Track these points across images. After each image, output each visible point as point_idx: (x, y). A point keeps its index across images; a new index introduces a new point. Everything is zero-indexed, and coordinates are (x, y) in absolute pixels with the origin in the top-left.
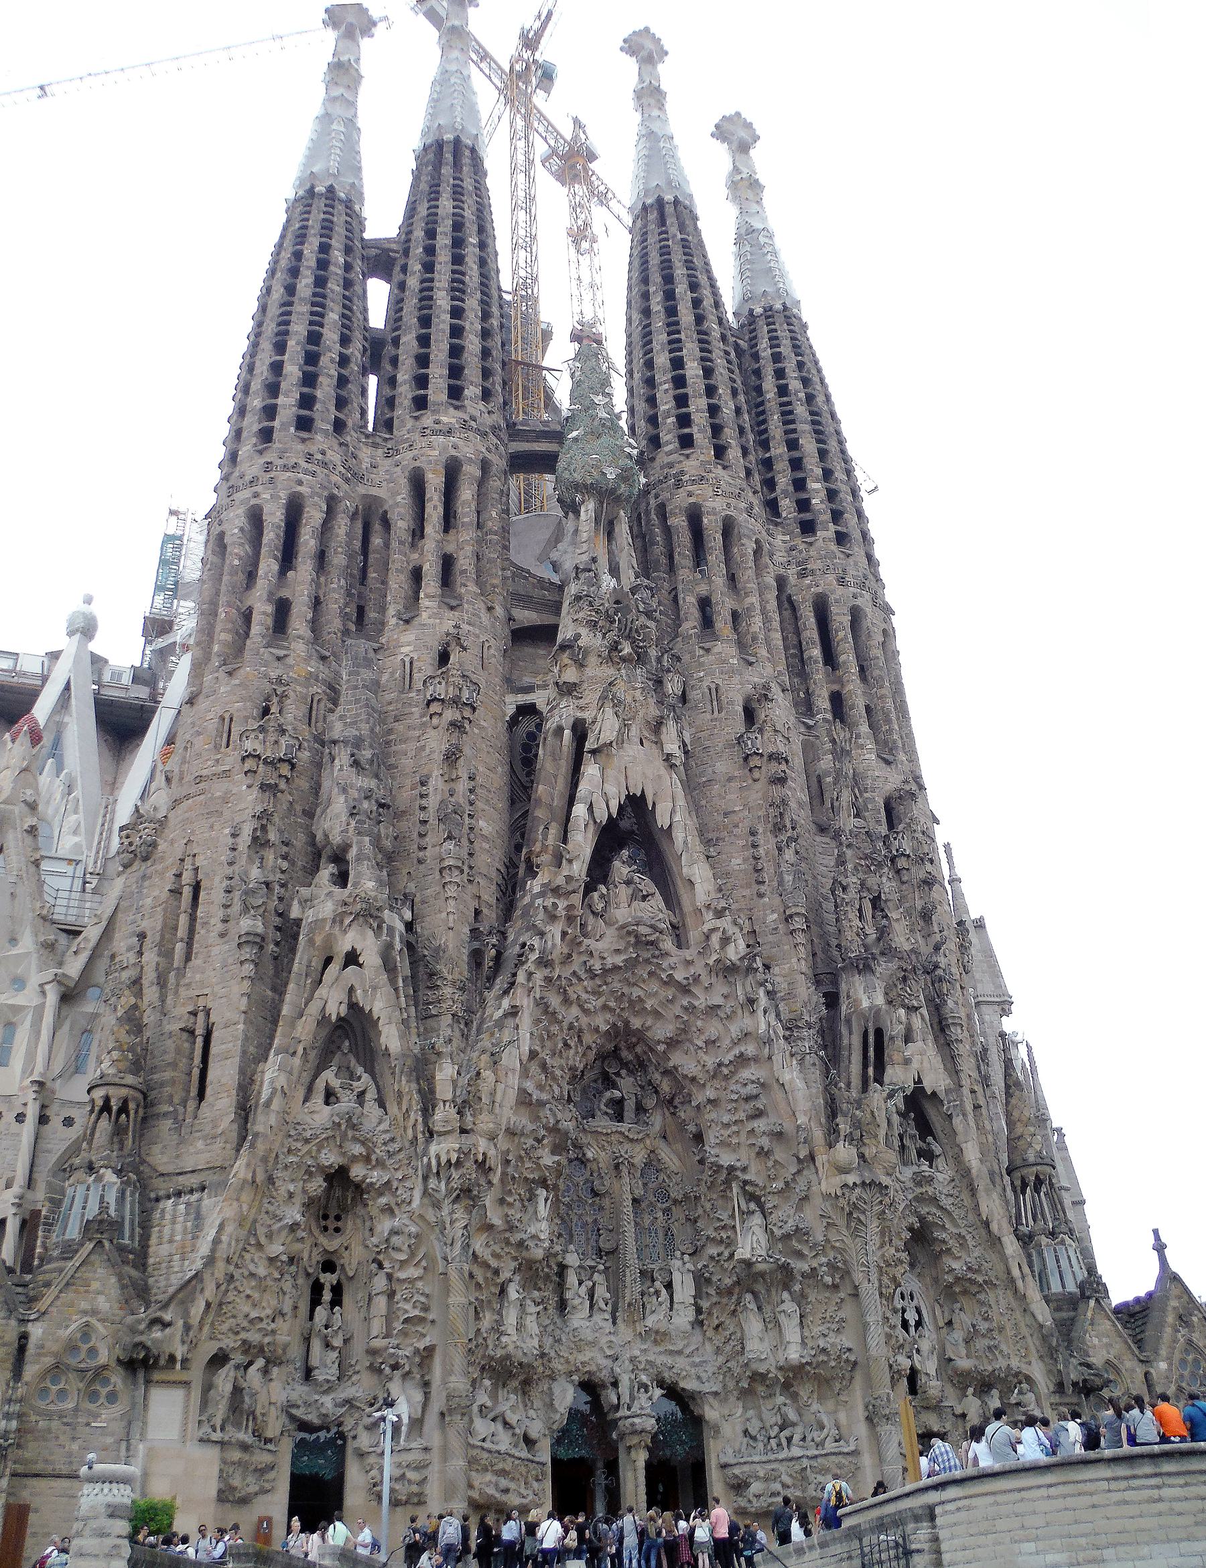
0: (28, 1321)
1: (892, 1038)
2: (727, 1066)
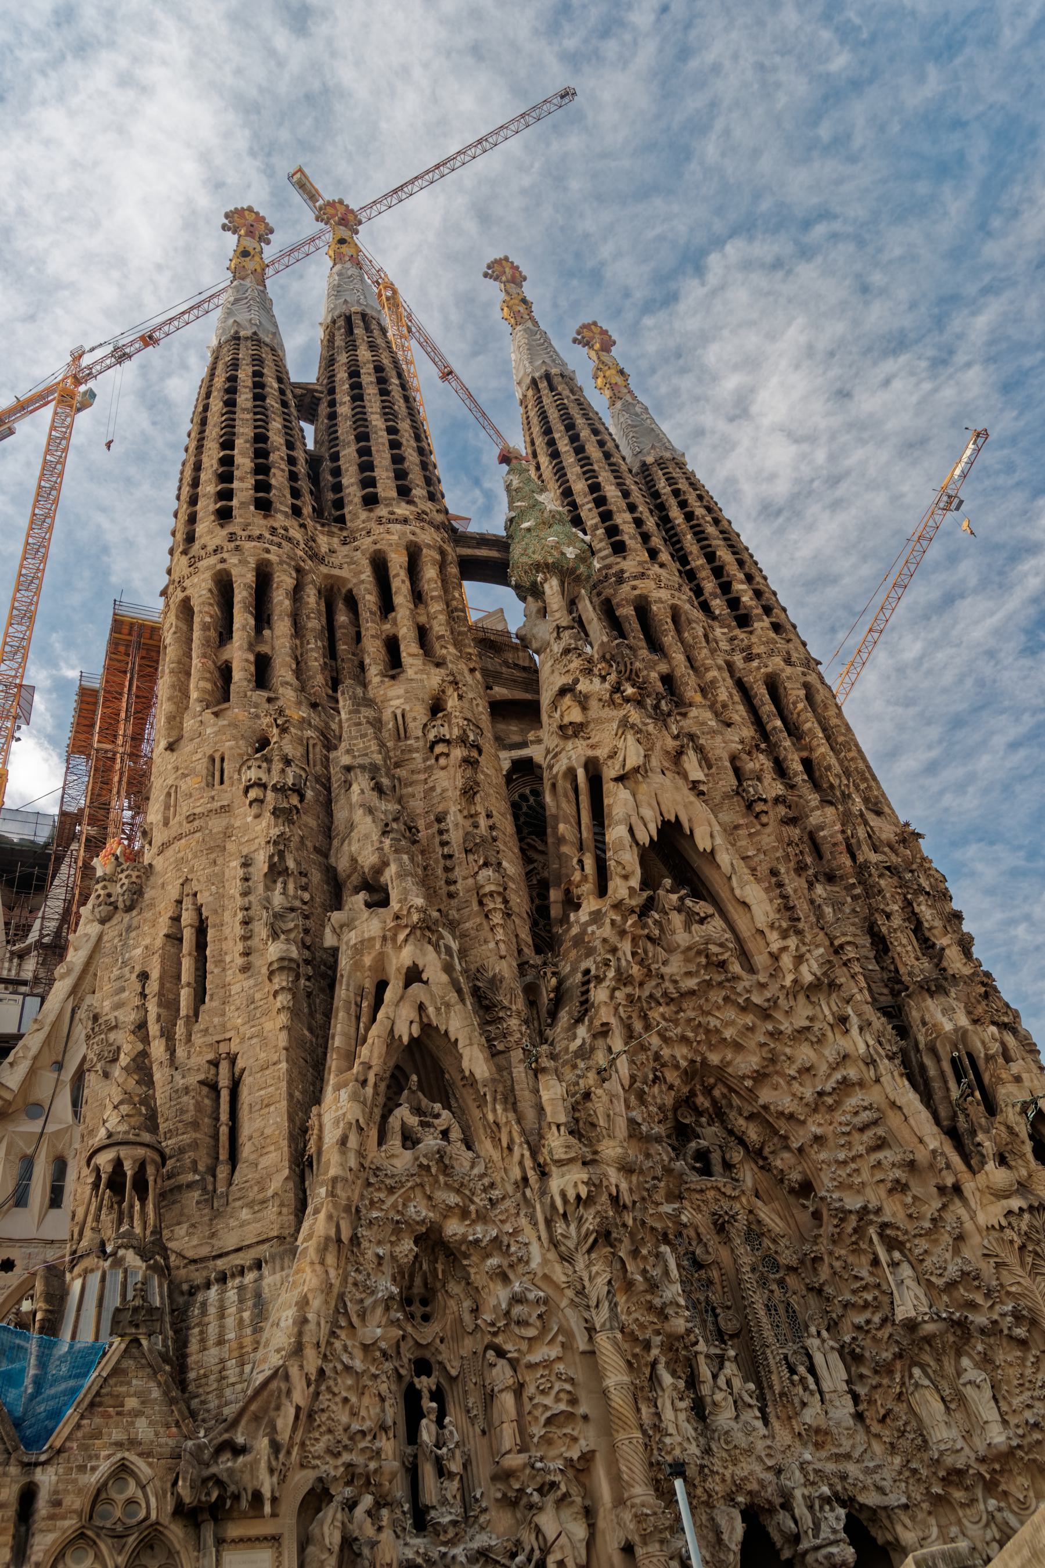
0: (37, 1464)
1: (989, 1058)
2: (830, 1094)
